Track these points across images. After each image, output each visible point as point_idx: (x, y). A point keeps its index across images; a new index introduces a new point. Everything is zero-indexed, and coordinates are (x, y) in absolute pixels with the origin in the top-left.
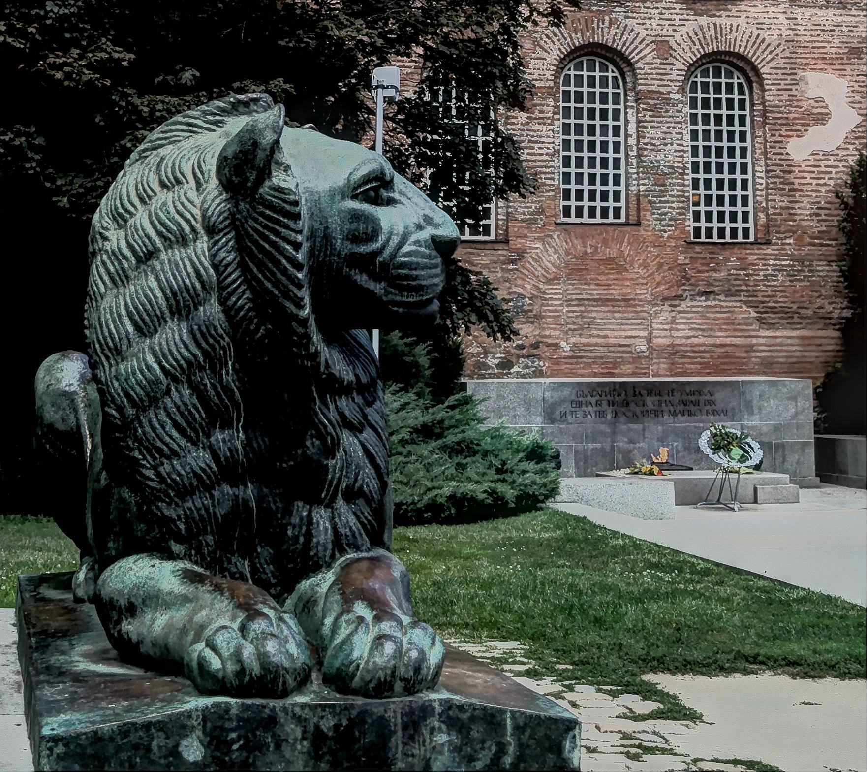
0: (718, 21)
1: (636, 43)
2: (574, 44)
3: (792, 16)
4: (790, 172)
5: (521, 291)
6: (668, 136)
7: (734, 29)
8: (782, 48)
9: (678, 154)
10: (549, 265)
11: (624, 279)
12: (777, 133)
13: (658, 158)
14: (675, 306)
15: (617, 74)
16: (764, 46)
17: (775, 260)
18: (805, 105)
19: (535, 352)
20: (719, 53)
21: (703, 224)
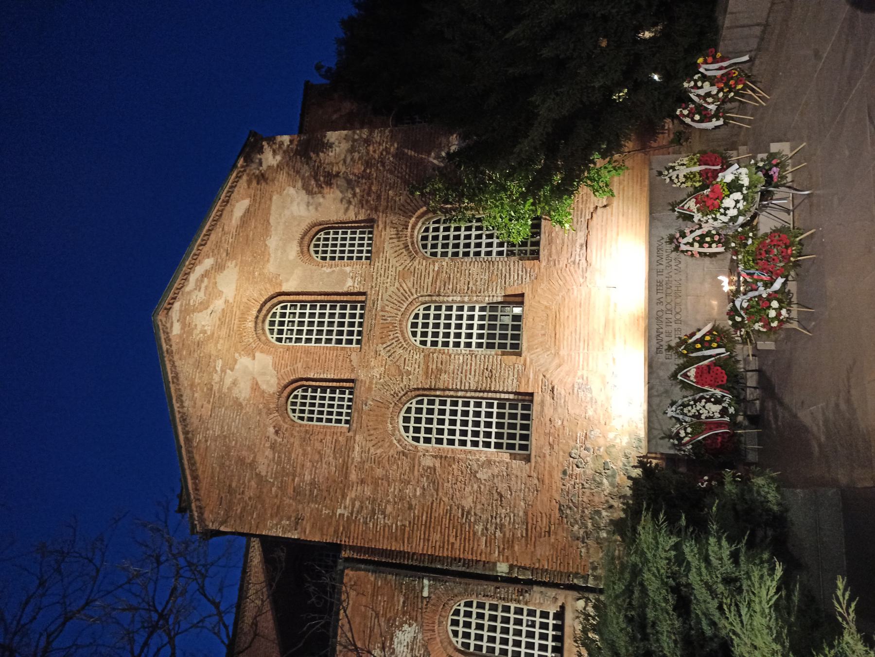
1: (400, 294)
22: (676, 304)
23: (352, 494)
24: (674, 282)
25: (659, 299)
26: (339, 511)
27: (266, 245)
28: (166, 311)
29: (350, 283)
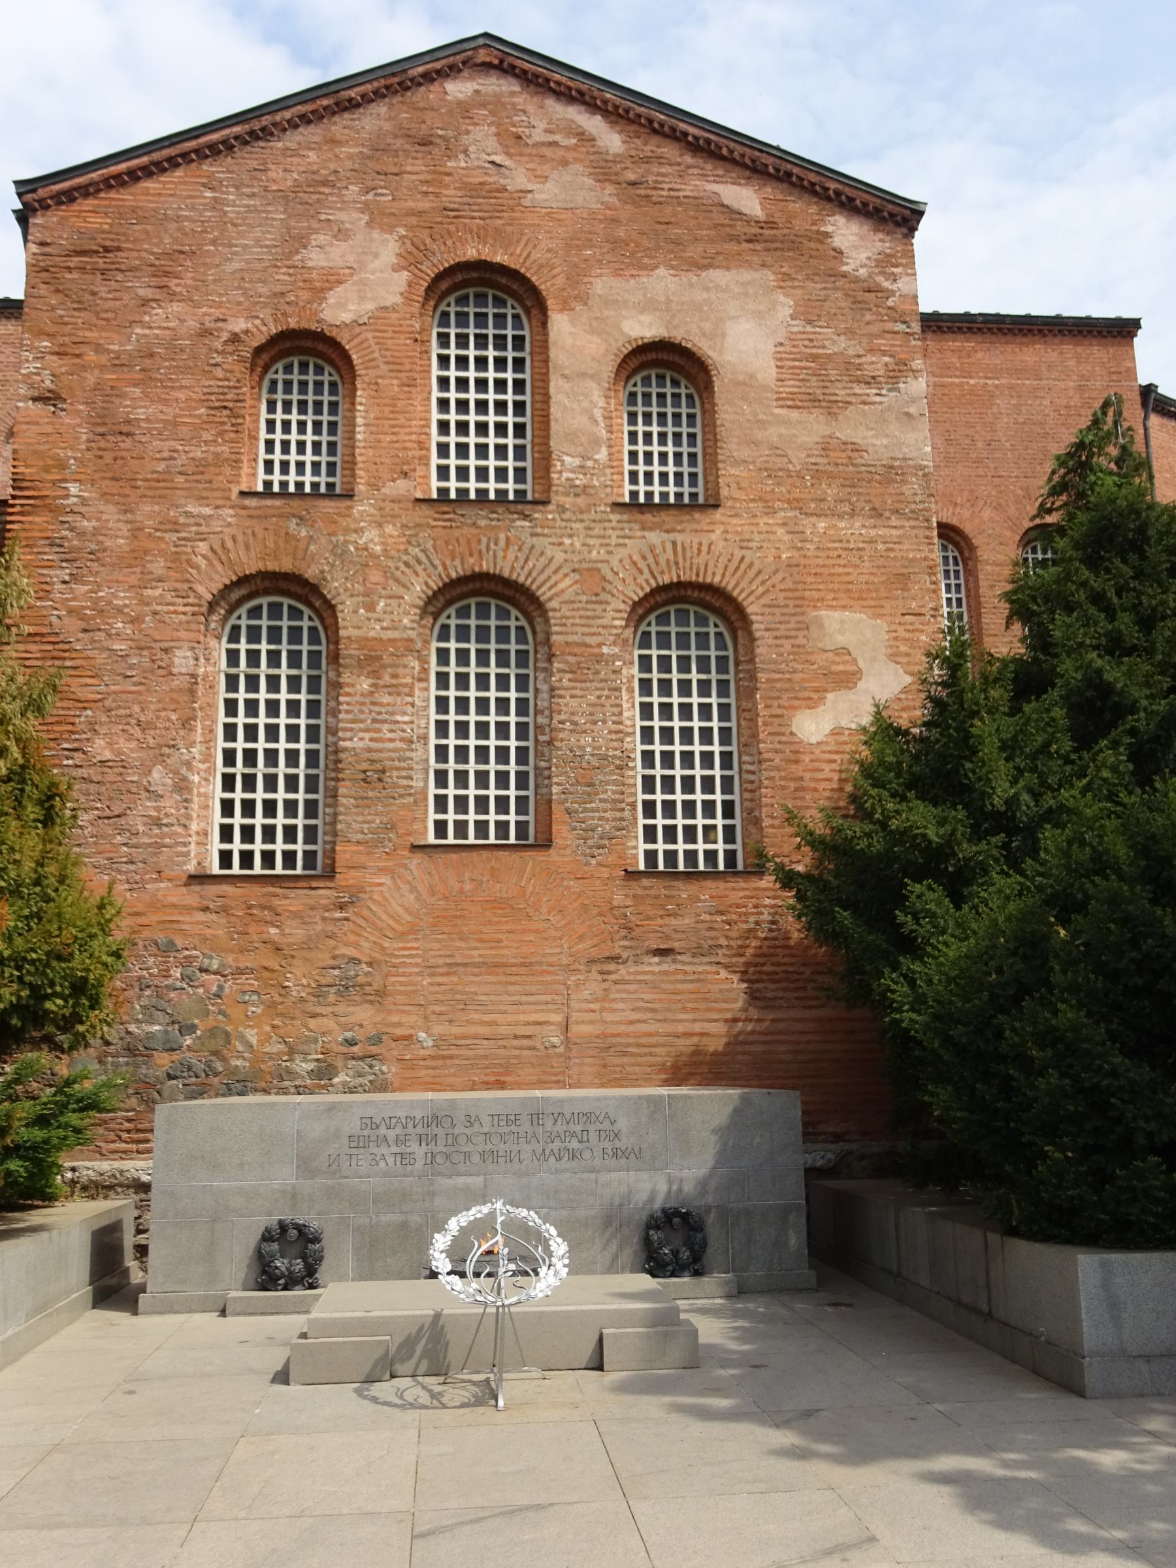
0: (679, 538)
2: (448, 575)
3: (797, 529)
4: (797, 762)
5: (351, 952)
6: (598, 709)
7: (704, 549)
8: (780, 576)
9: (614, 736)
10: (401, 911)
11: (523, 931)
12: (775, 703)
13: (582, 742)
14: (609, 973)
15: (523, 622)
16: (751, 573)
17: (774, 898)
18: (820, 659)
19: (374, 1050)
20: (680, 585)
21: (661, 846)
22: (467, 1155)
23: (110, 512)
24: (515, 1148)
25: (478, 1119)
26: (74, 489)
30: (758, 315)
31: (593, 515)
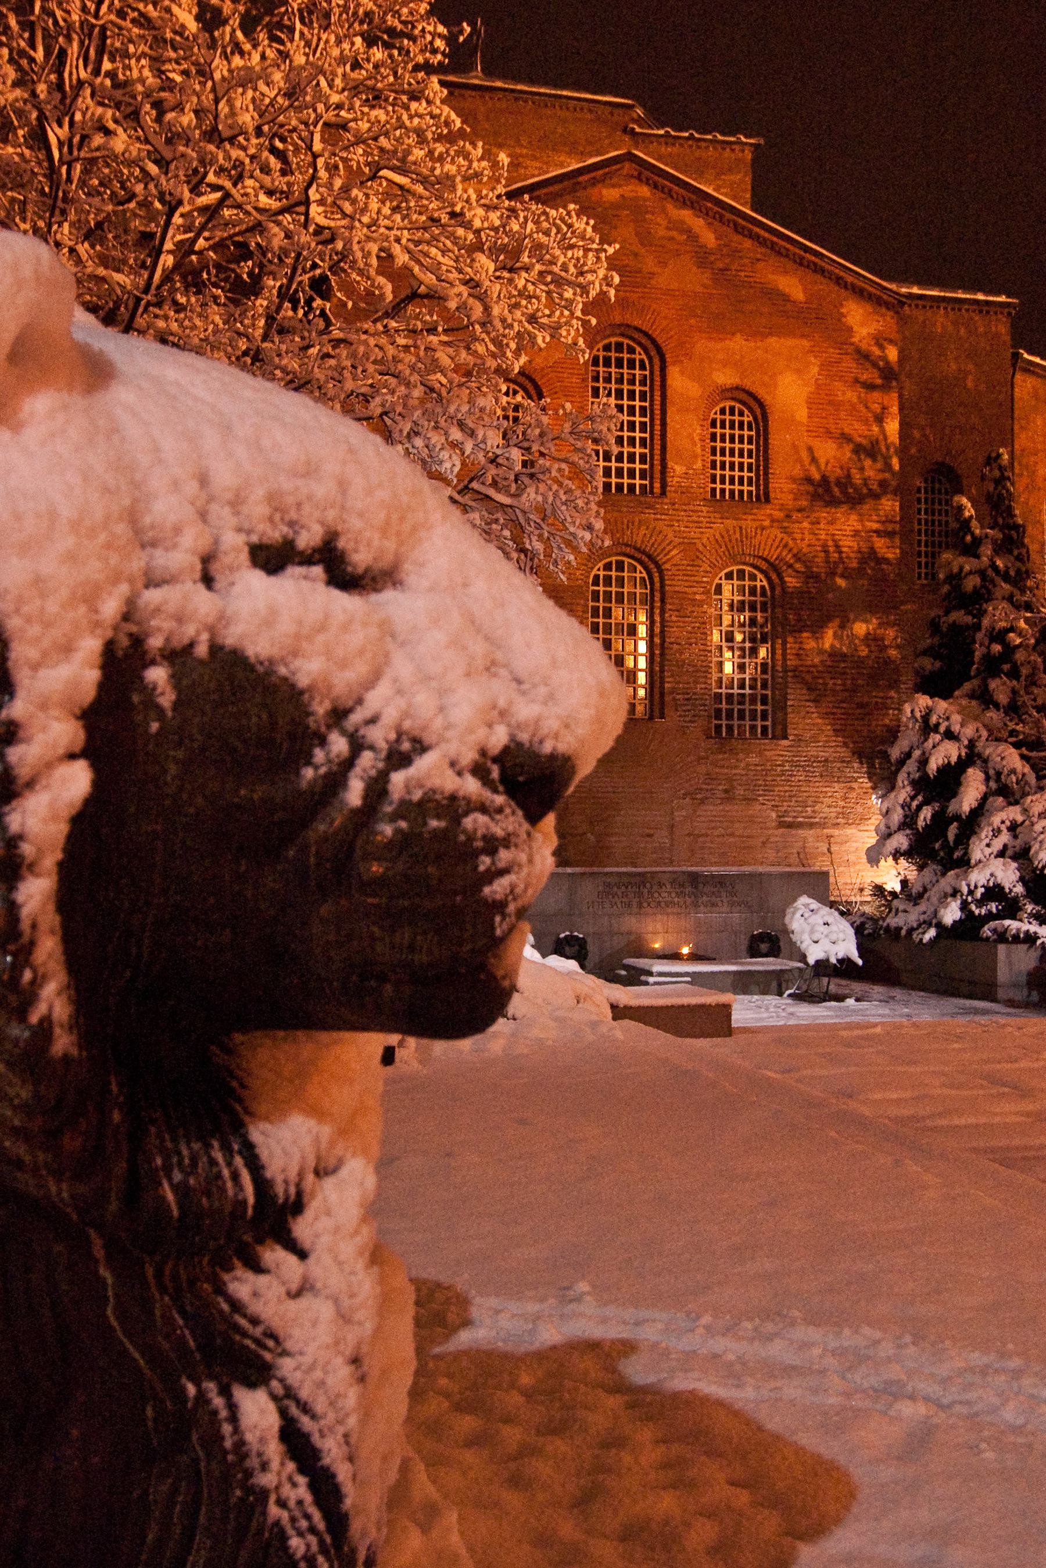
0: (743, 524)
27: (733, 334)
28: (636, 174)
29: (679, 469)
30: (798, 371)
31: (691, 507)
